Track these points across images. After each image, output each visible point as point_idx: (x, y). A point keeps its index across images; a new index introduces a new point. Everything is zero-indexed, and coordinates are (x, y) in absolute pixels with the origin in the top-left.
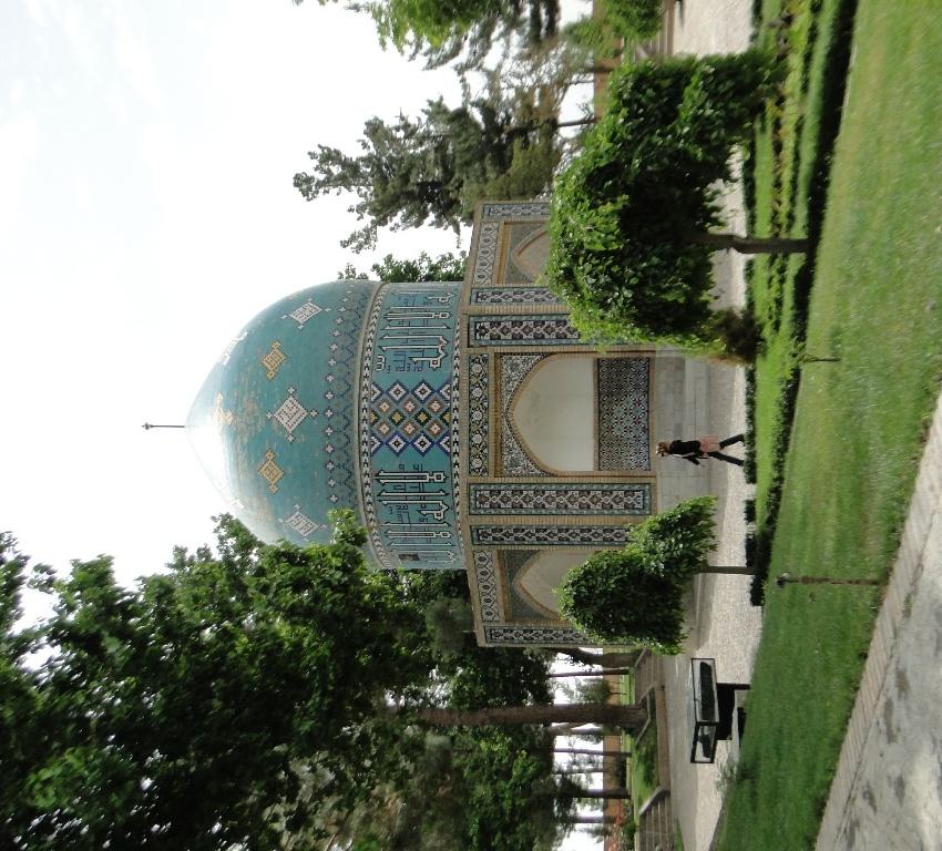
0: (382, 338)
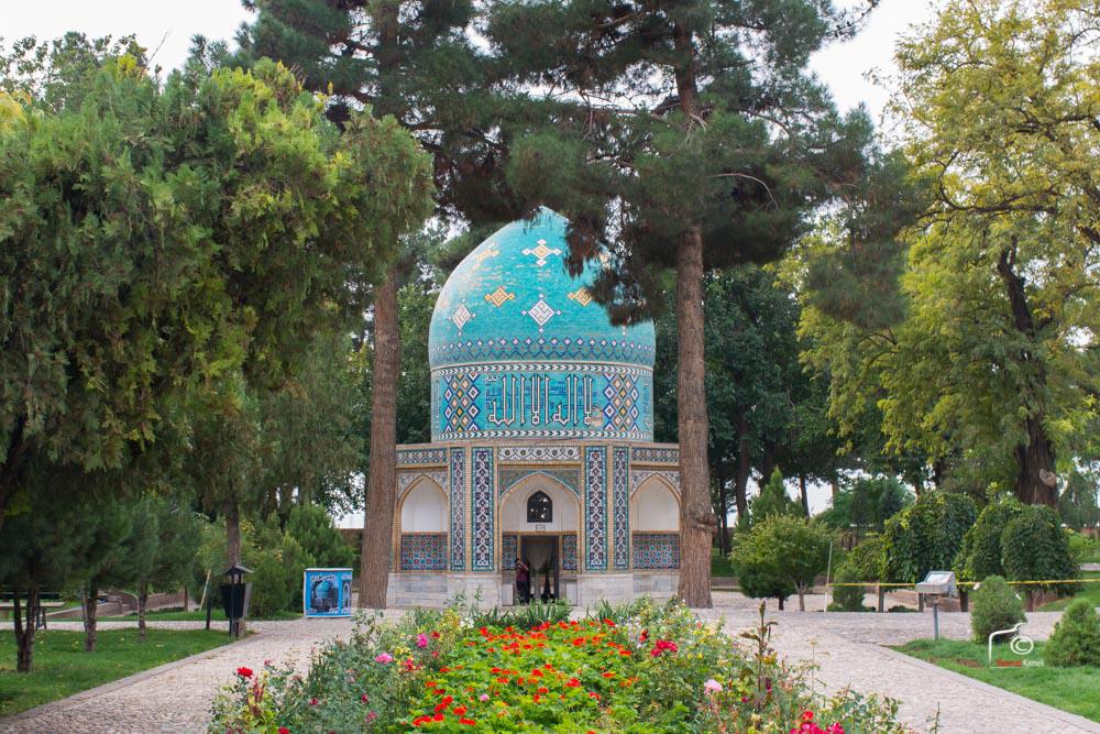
0: (513, 376)
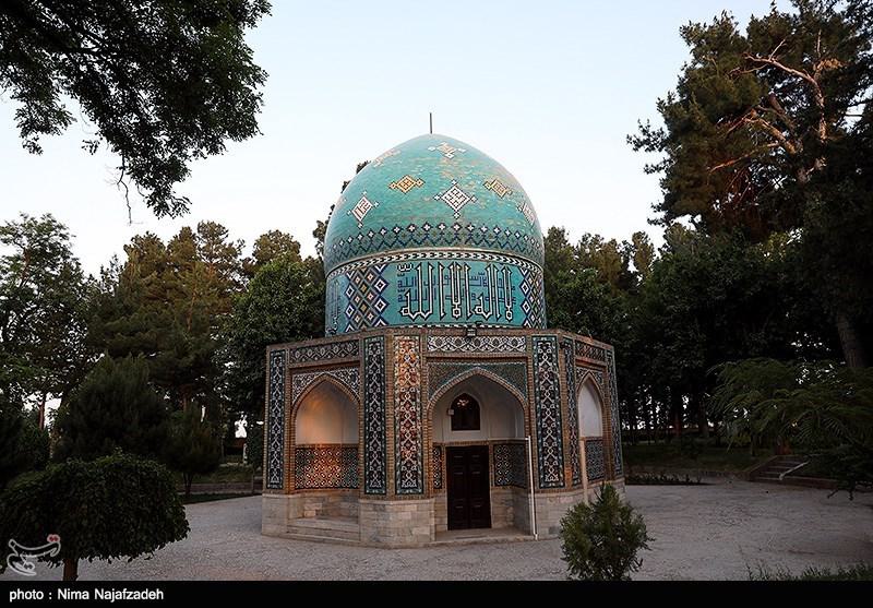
0: (429, 264)
